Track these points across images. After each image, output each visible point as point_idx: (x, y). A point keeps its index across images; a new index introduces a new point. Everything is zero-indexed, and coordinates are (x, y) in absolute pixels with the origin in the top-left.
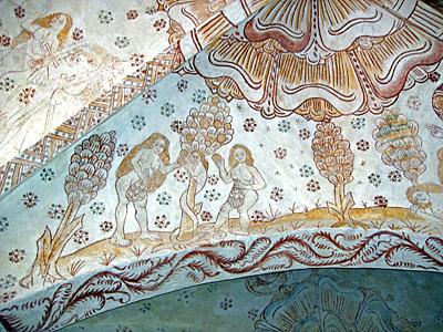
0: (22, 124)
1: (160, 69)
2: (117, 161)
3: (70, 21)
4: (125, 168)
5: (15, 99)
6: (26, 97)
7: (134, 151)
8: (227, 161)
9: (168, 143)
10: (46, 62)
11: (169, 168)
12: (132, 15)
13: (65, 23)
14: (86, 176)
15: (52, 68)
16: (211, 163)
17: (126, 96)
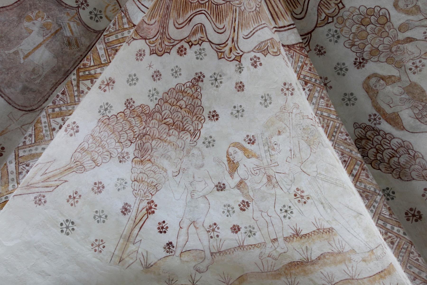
0: (331, 207)
1: (306, 68)
2: (385, 126)
3: (236, 145)
4: (395, 120)
5: (303, 208)
6: (302, 197)
7: (379, 109)
8: (410, 17)
9: (375, 75)
10: (271, 173)
11: (404, 78)
12: (240, 87)
13: (237, 149)
14: (396, 159)
15: (278, 169)
16: (409, 34)
17: (327, 105)
